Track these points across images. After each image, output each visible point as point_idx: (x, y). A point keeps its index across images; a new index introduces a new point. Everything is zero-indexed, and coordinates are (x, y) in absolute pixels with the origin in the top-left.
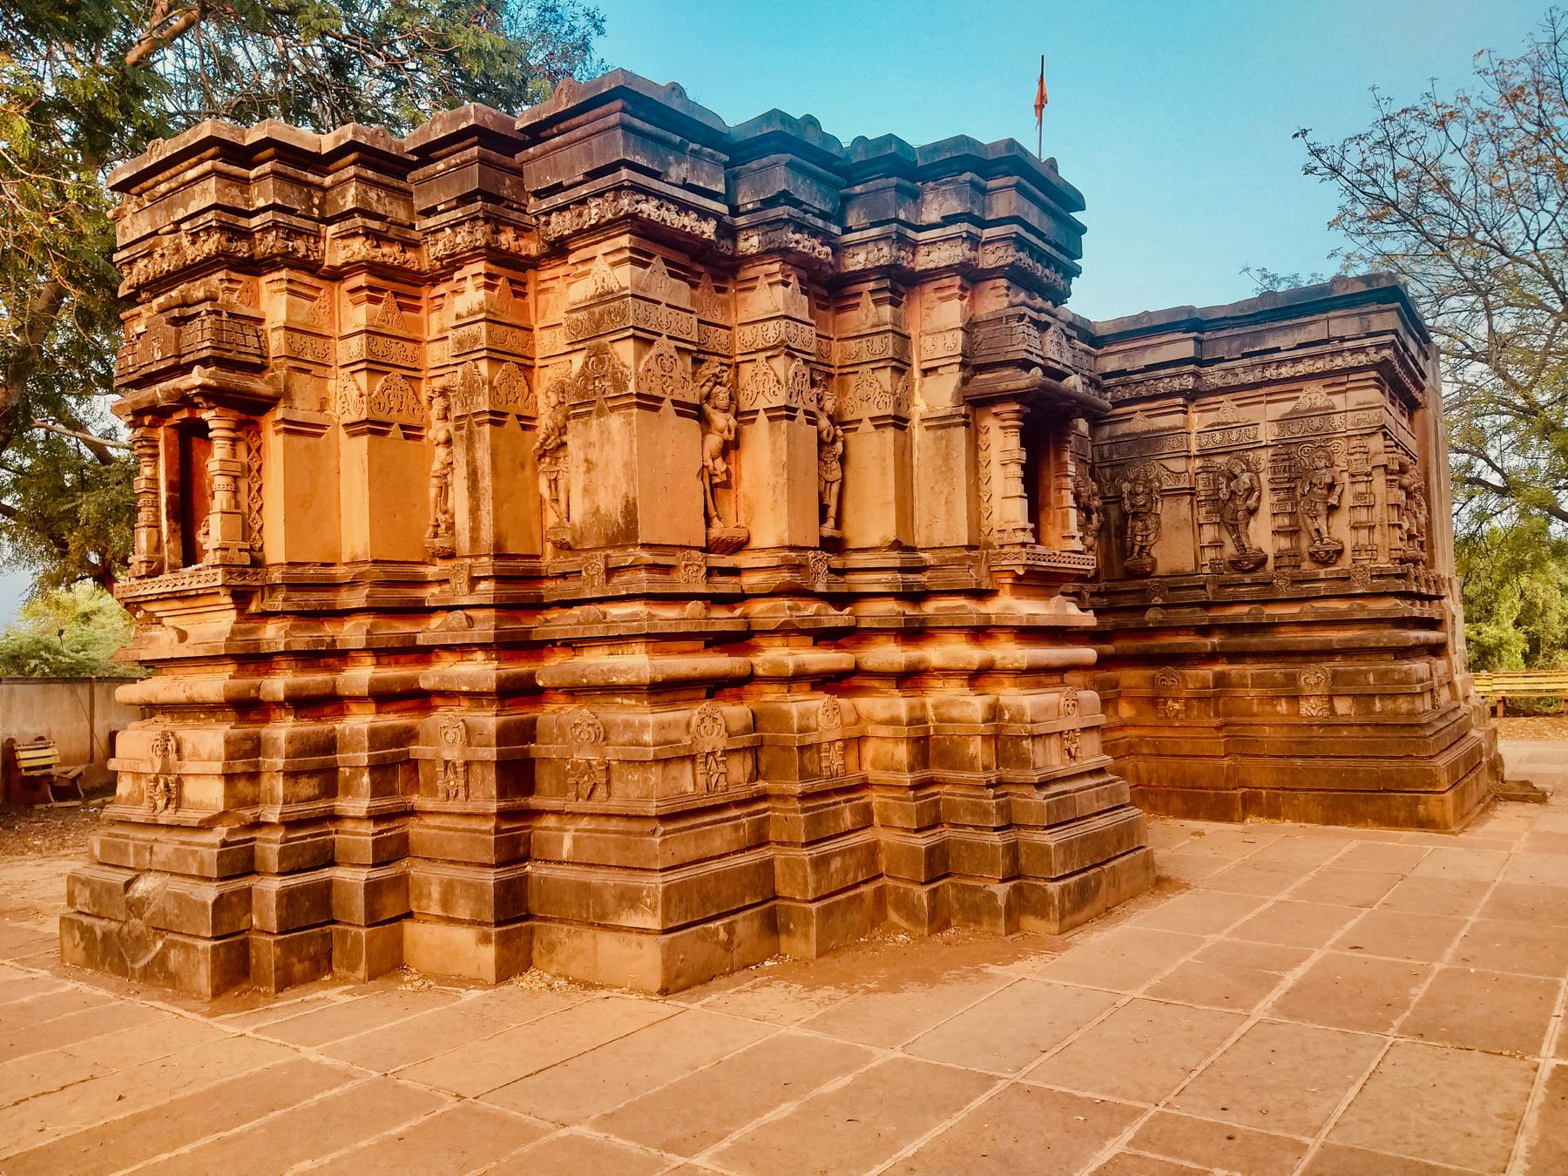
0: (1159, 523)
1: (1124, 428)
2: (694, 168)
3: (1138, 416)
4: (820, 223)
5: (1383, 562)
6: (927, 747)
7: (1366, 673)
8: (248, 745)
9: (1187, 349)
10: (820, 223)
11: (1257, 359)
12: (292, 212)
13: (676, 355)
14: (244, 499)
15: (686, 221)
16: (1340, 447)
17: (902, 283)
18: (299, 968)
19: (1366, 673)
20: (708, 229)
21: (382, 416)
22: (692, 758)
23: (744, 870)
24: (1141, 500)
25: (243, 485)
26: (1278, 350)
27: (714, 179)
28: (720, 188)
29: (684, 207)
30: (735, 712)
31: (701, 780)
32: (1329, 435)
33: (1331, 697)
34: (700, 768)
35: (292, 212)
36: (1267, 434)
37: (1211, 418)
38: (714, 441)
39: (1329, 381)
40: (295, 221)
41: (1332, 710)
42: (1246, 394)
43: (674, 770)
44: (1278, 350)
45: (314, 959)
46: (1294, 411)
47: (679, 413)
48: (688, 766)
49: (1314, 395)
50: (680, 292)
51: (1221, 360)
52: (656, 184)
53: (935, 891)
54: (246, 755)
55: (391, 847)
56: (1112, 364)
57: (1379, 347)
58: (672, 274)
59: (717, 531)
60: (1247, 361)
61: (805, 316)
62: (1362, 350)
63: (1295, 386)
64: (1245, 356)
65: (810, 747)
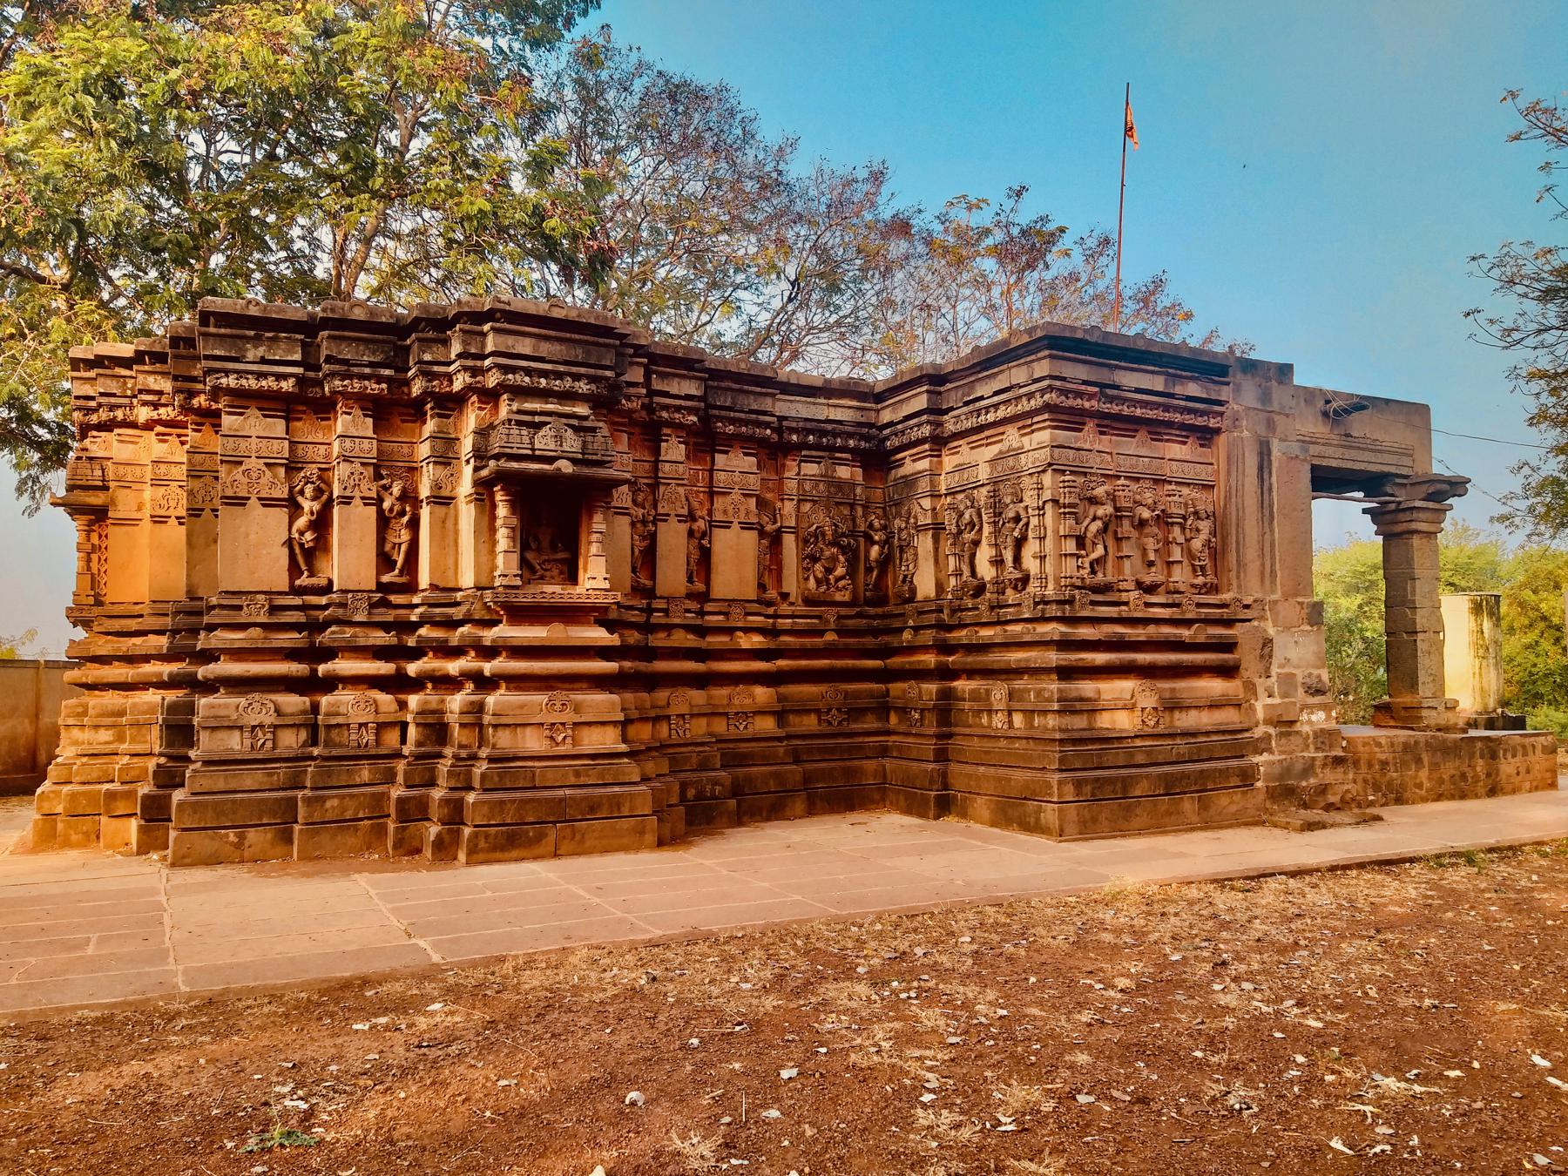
0: (916, 555)
1: (902, 471)
2: (270, 348)
3: (907, 461)
4: (367, 370)
5: (1050, 591)
6: (436, 729)
7: (1029, 691)
8: (80, 710)
9: (921, 402)
10: (367, 370)
11: (971, 407)
12: (114, 395)
14: (94, 565)
15: (264, 383)
16: (1027, 482)
17: (451, 404)
18: (74, 837)
19: (1029, 691)
20: (288, 385)
21: (163, 512)
22: (241, 728)
23: (276, 800)
24: (904, 535)
25: (94, 557)
26: (982, 398)
27: (290, 351)
28: (297, 357)
29: (260, 375)
30: (293, 702)
31: (248, 742)
32: (1017, 473)
33: (1010, 713)
34: (246, 735)
35: (114, 395)
36: (983, 473)
37: (956, 460)
38: (302, 522)
39: (1020, 424)
40: (113, 400)
41: (1010, 722)
42: (974, 438)
43: (221, 735)
44: (982, 398)
45: (87, 834)
46: (1001, 452)
47: (264, 505)
48: (237, 733)
49: (1012, 436)
50: (278, 427)
51: (952, 409)
52: (231, 365)
53: (404, 828)
54: (79, 715)
55: (133, 773)
56: (886, 416)
57: (1043, 392)
58: (265, 416)
59: (304, 581)
60: (965, 409)
61: (370, 433)
62: (1030, 396)
63: (1001, 429)
64: (967, 404)
65: (339, 726)
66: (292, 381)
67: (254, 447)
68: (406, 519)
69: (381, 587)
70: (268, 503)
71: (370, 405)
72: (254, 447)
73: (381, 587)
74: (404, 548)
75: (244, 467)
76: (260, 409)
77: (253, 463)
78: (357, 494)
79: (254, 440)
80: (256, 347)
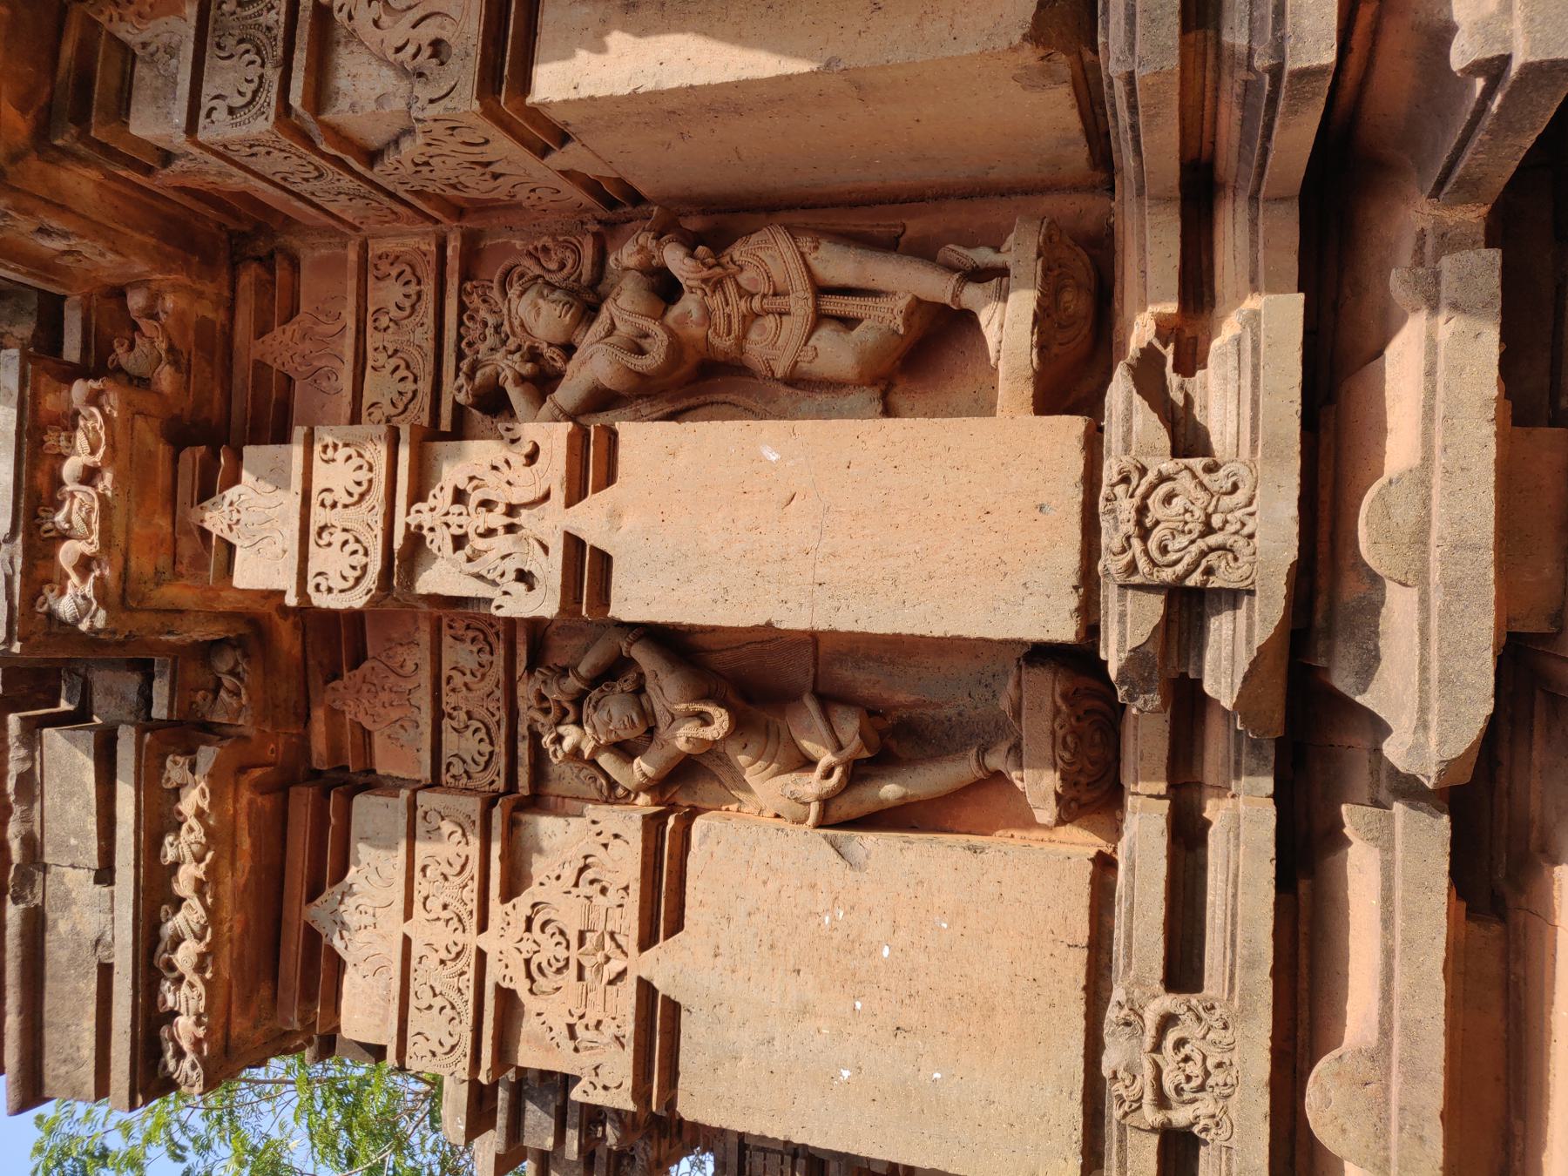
13: (523, 902)
47: (676, 926)
66: (175, 770)
67: (443, 936)
68: (675, 259)
69: (1069, 383)
70: (662, 911)
71: (193, 456)
72: (443, 936)
73: (1069, 383)
74: (838, 265)
75: (521, 986)
76: (315, 892)
77: (504, 943)
78: (552, 522)
79: (422, 930)
80: (67, 902)
